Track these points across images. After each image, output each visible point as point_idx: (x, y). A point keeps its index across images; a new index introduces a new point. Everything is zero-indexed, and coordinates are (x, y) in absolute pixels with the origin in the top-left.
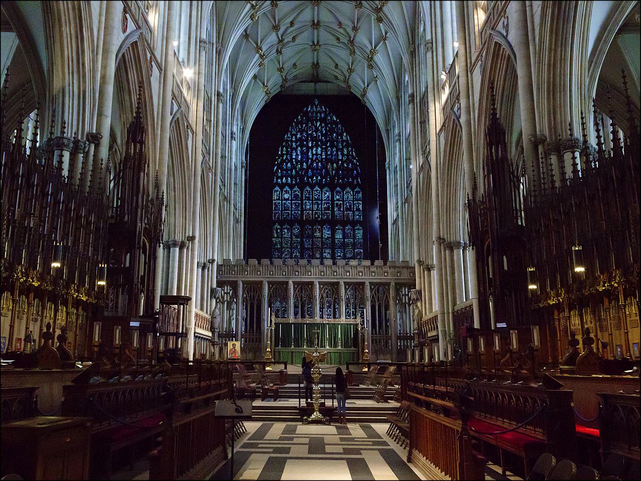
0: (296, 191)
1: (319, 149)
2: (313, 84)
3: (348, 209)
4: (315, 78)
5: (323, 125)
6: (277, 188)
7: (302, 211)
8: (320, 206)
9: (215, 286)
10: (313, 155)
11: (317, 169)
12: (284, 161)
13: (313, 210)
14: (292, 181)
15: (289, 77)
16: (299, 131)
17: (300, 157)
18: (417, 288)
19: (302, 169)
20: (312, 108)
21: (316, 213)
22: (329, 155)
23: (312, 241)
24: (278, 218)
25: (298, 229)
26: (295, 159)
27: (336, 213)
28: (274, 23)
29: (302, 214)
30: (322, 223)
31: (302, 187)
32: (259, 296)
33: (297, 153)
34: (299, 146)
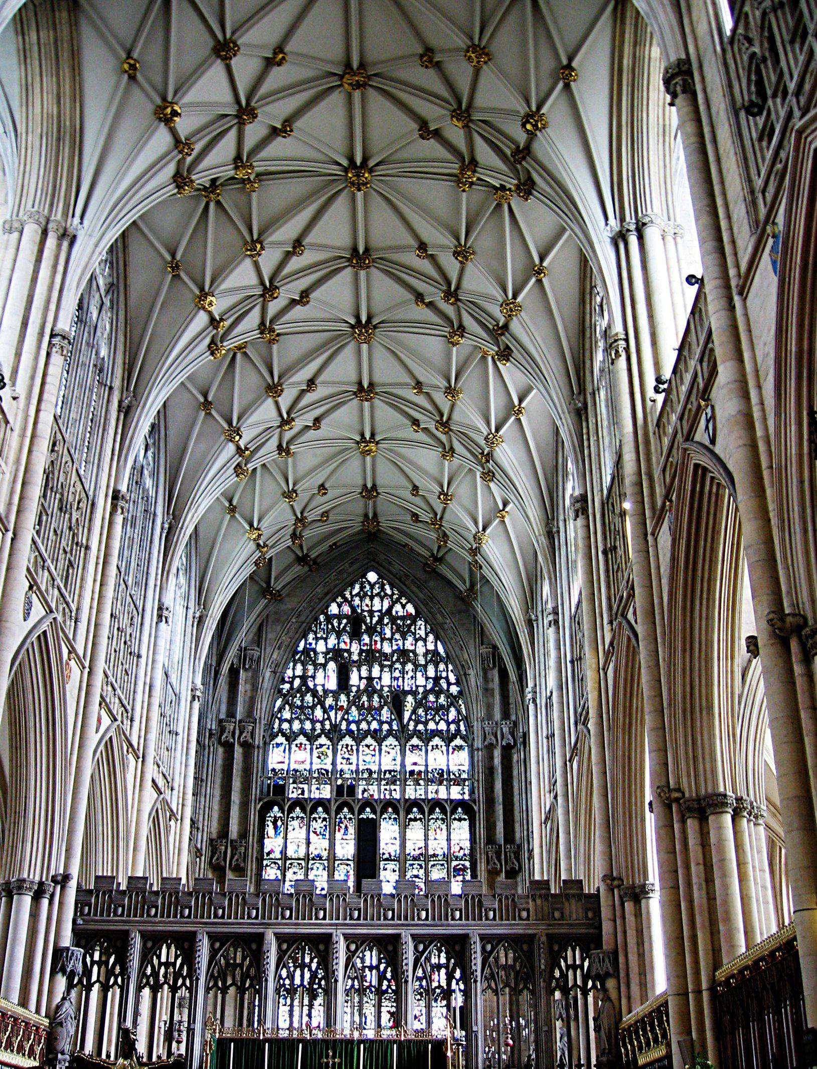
9: (67, 940)
11: (370, 709)
15: (311, 516)
18: (607, 944)
28: (270, 381)
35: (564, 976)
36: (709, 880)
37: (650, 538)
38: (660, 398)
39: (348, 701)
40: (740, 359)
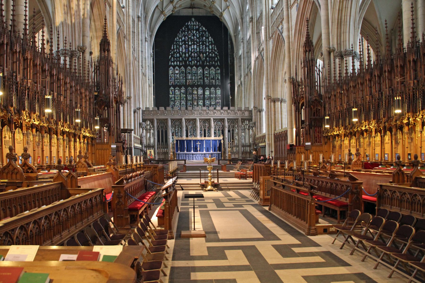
0: (182, 69)
1: (195, 46)
2: (191, 9)
3: (212, 79)
4: (192, 7)
5: (197, 32)
6: (171, 68)
7: (186, 80)
8: (196, 77)
10: (192, 49)
11: (194, 57)
12: (175, 53)
13: (192, 80)
14: (180, 64)
15: (177, 6)
16: (184, 36)
17: (184, 50)
19: (185, 57)
20: (191, 23)
21: (194, 81)
22: (201, 49)
23: (192, 96)
24: (172, 84)
25: (184, 90)
26: (182, 51)
27: (206, 81)
29: (186, 82)
30: (198, 86)
31: (186, 66)
32: (166, 126)
33: (182, 48)
34: (184, 44)
35: (244, 127)
36: (275, 114)
37: (268, 41)
38: (272, 10)
39: (189, 55)
40: (289, 23)
